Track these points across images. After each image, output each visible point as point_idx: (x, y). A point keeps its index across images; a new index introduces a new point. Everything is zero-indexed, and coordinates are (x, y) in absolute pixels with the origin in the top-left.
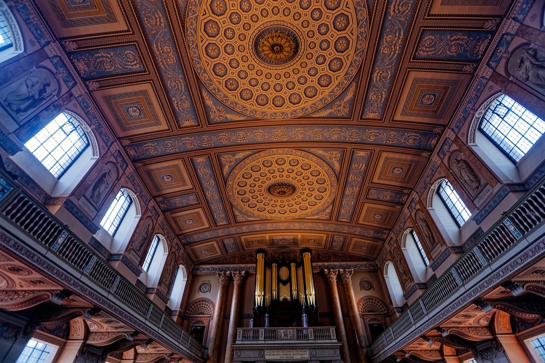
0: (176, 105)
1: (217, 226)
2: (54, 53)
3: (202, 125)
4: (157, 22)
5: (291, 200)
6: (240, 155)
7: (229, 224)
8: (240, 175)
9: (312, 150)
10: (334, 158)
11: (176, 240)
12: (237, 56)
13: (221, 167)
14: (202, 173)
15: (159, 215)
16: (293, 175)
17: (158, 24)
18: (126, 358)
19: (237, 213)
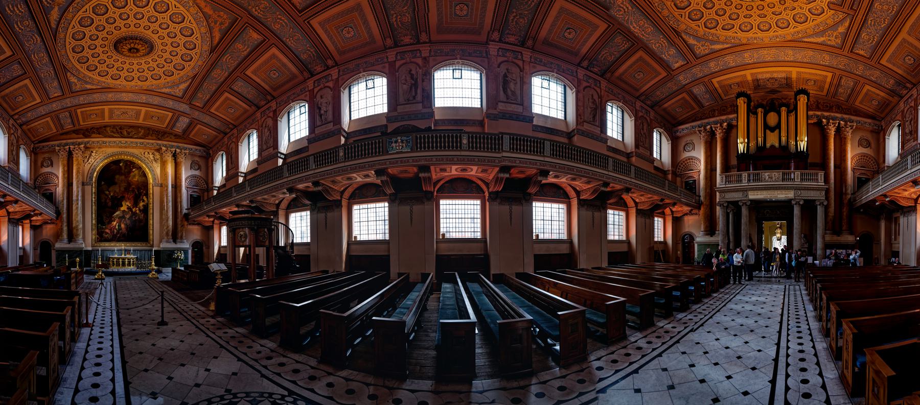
1: (50, 99)
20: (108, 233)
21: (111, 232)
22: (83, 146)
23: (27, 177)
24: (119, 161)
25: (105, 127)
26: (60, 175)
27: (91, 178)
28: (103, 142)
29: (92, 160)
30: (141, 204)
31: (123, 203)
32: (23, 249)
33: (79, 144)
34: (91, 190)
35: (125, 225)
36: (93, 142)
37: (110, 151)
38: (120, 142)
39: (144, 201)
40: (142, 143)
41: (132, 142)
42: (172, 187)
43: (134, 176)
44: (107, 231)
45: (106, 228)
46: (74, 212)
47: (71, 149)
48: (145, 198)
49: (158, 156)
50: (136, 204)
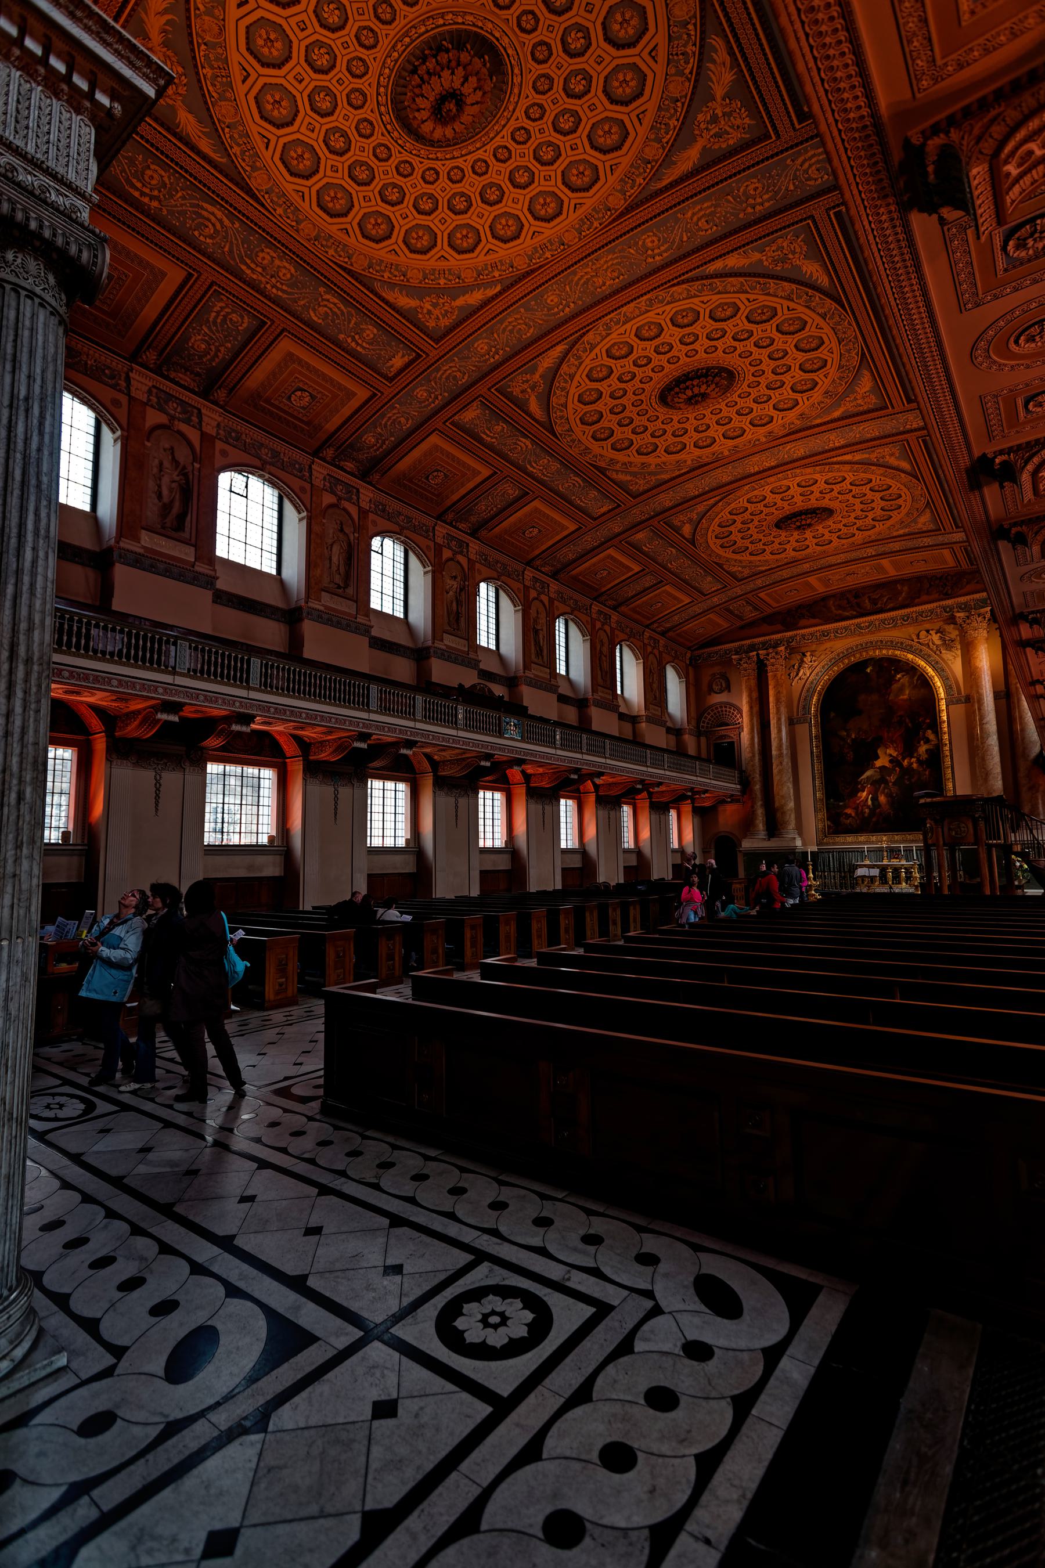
0: (353, 344)
2: (145, 389)
3: (424, 352)
4: (214, 225)
5: (738, 400)
6: (547, 362)
7: (619, 506)
8: (573, 404)
9: (711, 268)
10: (791, 256)
11: (529, 573)
12: (385, 173)
13: (522, 405)
14: (492, 438)
15: (468, 545)
16: (703, 343)
17: (218, 226)
18: (515, 781)
19: (621, 477)
20: (850, 816)
21: (856, 813)
22: (783, 648)
23: (682, 719)
24: (864, 664)
25: (825, 599)
26: (745, 708)
27: (806, 708)
28: (824, 634)
29: (805, 672)
30: (923, 749)
31: (879, 752)
32: (681, 851)
33: (776, 645)
34: (809, 732)
35: (889, 796)
36: (803, 636)
37: (840, 645)
38: (858, 626)
39: (927, 741)
40: (908, 616)
41: (883, 621)
42: (997, 696)
43: (901, 690)
44: (849, 811)
45: (846, 807)
46: (776, 778)
47: (762, 657)
48: (930, 734)
49: (953, 633)
50: (909, 750)
